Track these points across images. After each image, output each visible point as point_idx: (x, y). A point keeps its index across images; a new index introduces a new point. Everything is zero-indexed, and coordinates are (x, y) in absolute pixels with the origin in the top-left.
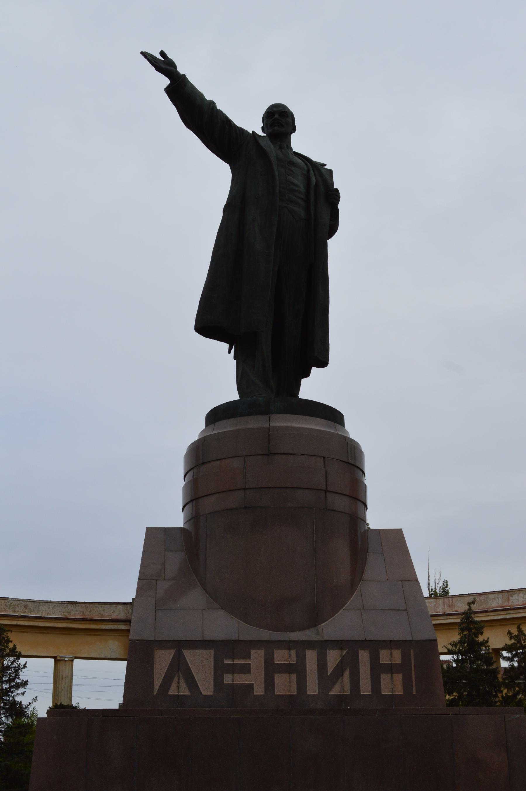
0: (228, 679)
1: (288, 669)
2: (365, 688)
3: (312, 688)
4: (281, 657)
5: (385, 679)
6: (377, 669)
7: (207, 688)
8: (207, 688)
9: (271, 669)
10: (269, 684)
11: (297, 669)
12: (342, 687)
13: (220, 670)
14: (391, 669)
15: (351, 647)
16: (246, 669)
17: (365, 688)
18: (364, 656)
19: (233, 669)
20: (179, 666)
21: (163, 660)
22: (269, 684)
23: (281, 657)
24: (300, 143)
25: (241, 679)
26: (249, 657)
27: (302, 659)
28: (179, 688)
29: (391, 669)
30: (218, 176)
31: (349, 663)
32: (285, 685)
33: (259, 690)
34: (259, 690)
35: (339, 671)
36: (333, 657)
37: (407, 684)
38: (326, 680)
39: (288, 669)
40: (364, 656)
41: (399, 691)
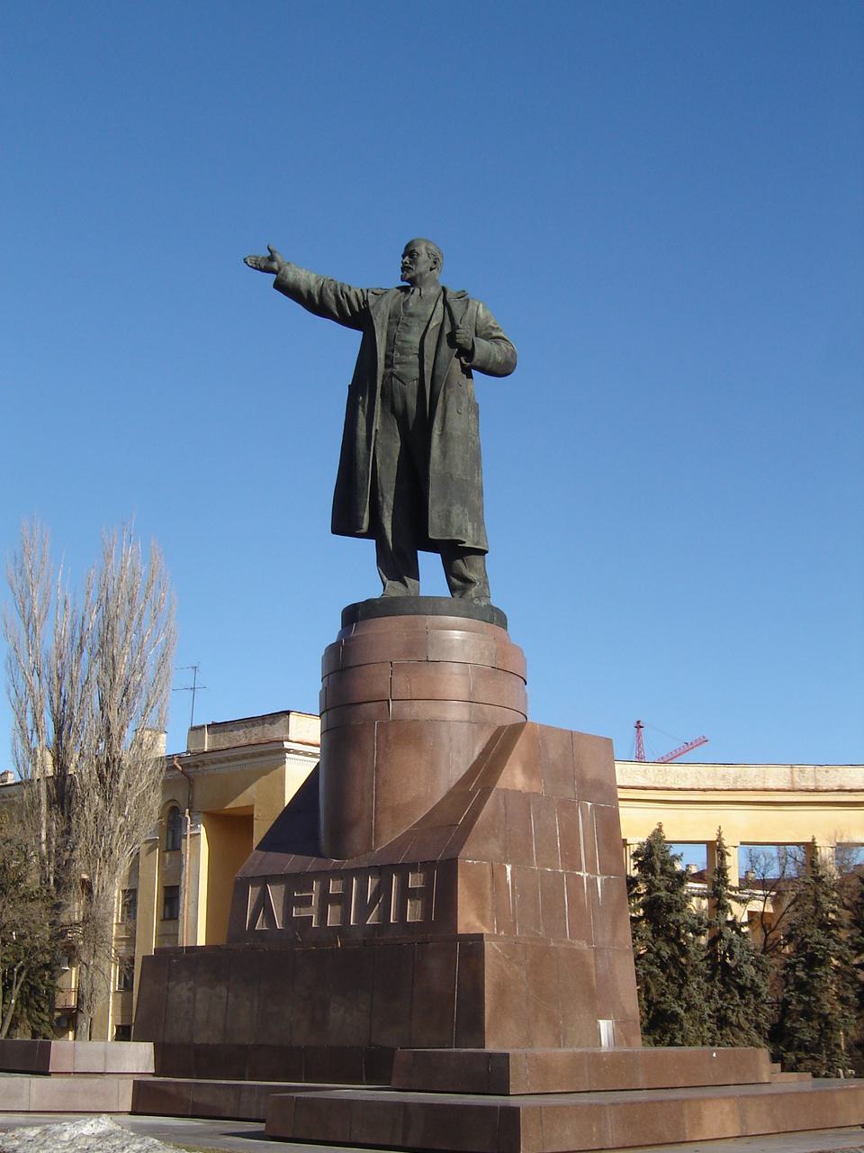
4: (334, 887)
6: (406, 894)
9: (326, 898)
10: (323, 916)
11: (343, 900)
13: (289, 902)
15: (383, 871)
16: (306, 902)
20: (263, 901)
21: (253, 893)
22: (323, 916)
23: (334, 887)
25: (304, 912)
26: (311, 889)
27: (348, 887)
28: (260, 925)
31: (383, 889)
36: (371, 883)
37: (426, 911)
38: (364, 910)
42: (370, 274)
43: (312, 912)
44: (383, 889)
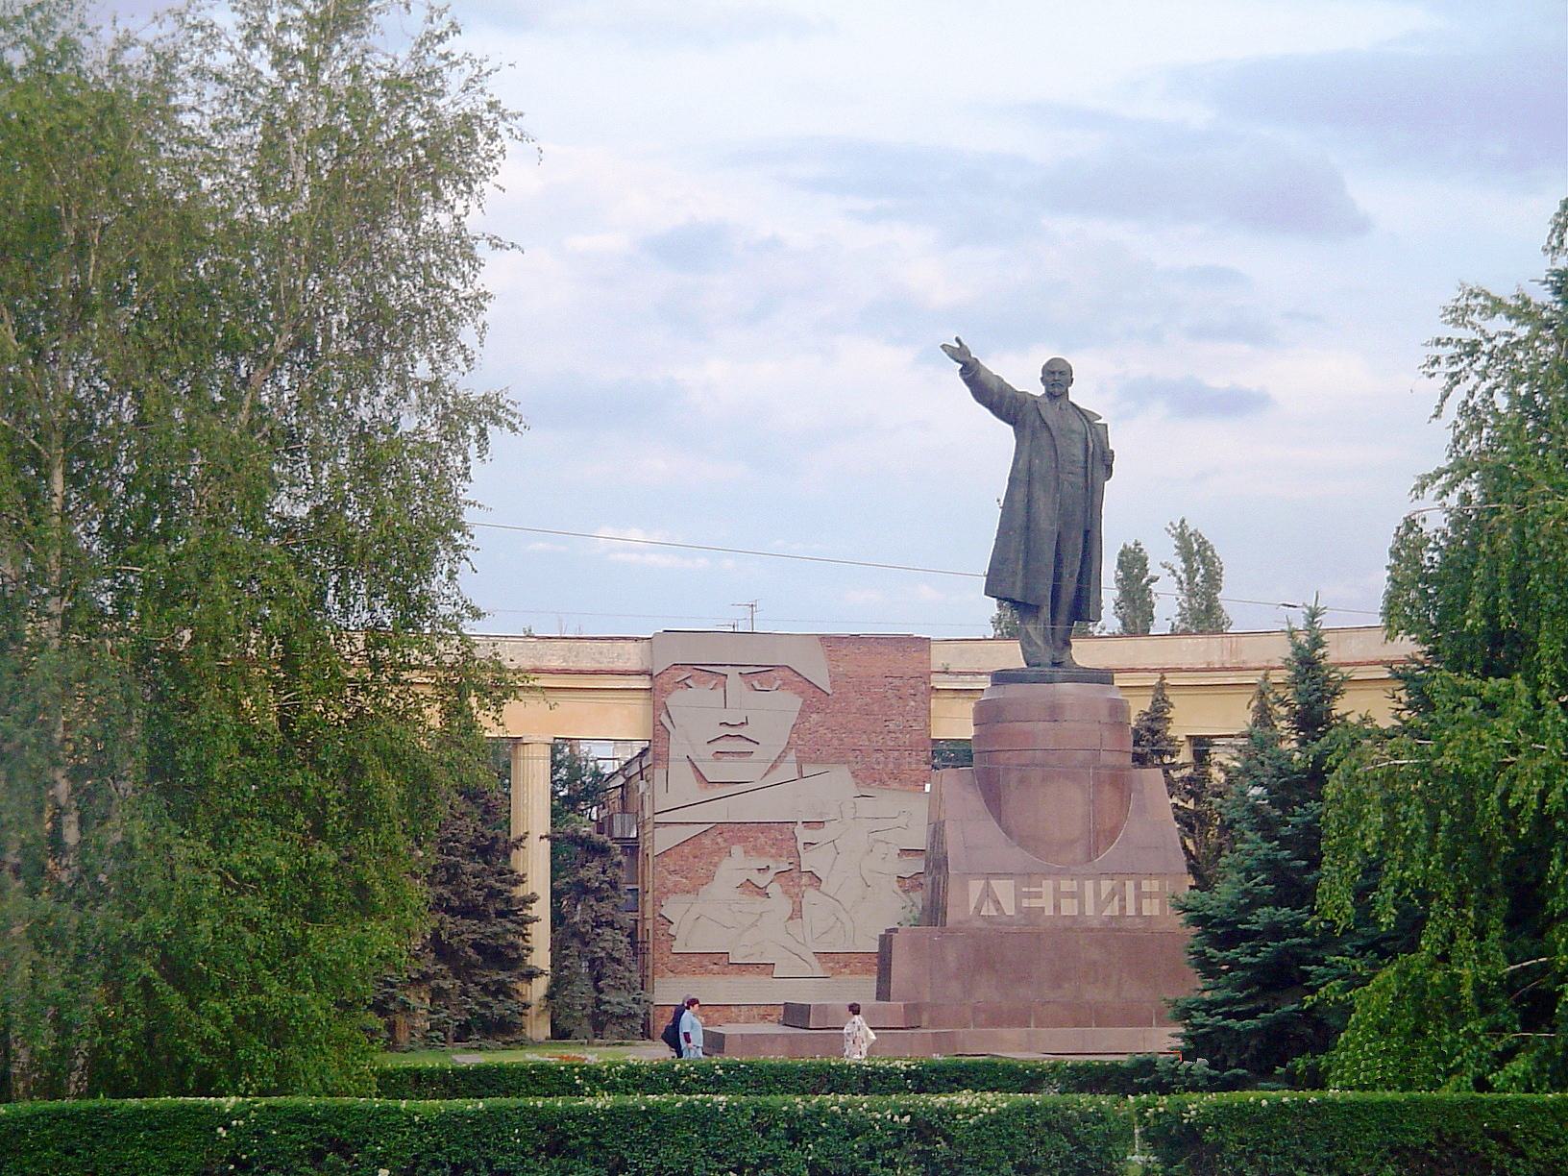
0: (1025, 903)
1: (1072, 895)
2: (1131, 911)
3: (1090, 911)
4: (1066, 885)
5: (1145, 902)
6: (1139, 896)
7: (1010, 909)
8: (1010, 909)
9: (1058, 895)
10: (1057, 907)
11: (1078, 896)
12: (1112, 910)
13: (1019, 896)
14: (1151, 895)
16: (1038, 895)
17: (1131, 911)
18: (1130, 885)
19: (1029, 895)
20: (987, 893)
22: (1057, 907)
24: (1077, 395)
25: (1035, 903)
27: (1081, 887)
28: (989, 910)
29: (1151, 895)
30: (1002, 437)
32: (1069, 908)
33: (1049, 912)
34: (1049, 912)
35: (1112, 894)
38: (1099, 905)
39: (1072, 895)
40: (1130, 885)
41: (1156, 912)
42: (1025, 378)
43: (1046, 904)
44: (1118, 893)
